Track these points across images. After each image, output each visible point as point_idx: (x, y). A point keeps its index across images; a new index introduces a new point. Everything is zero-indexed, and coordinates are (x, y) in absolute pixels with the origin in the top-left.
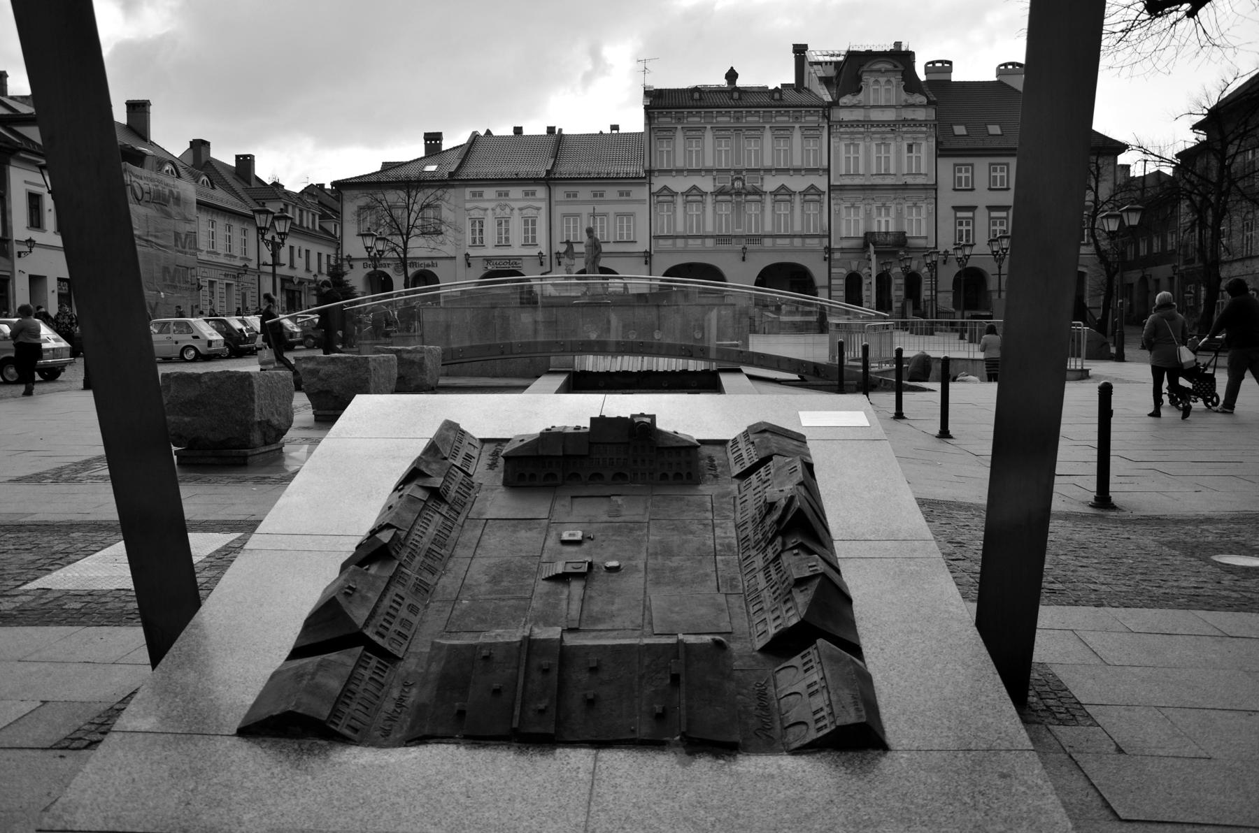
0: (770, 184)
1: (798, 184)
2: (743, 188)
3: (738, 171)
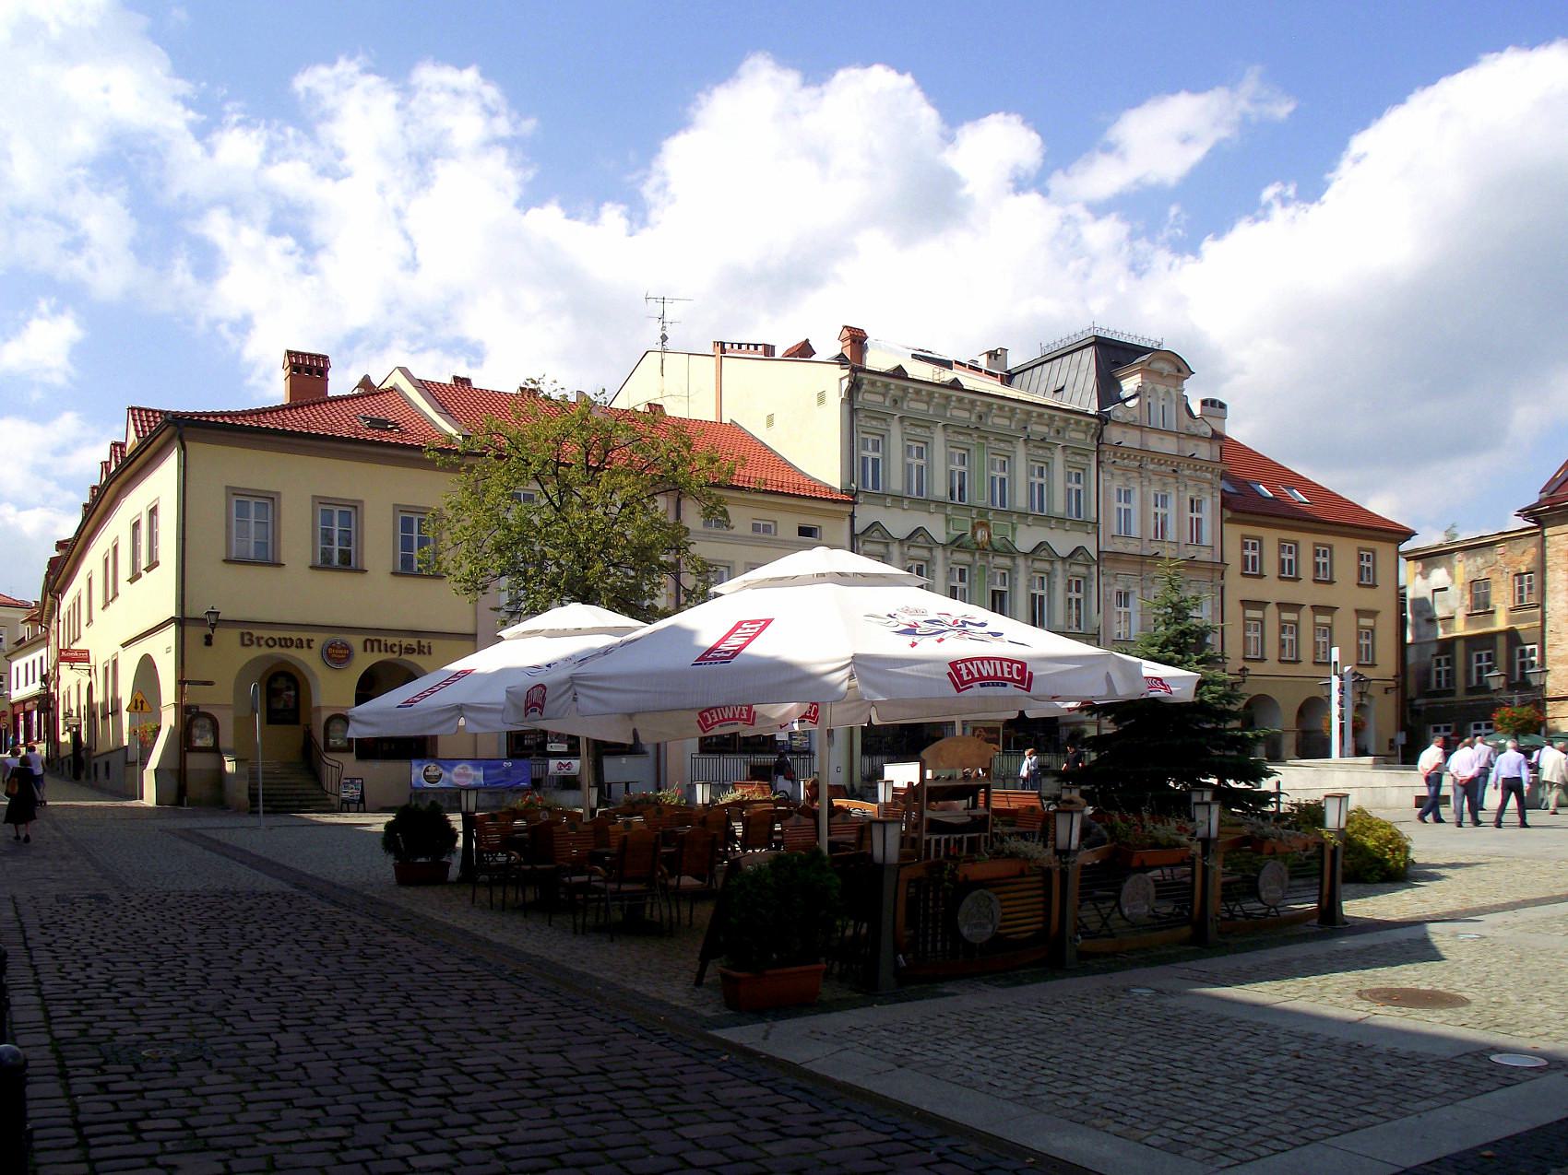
0: (1026, 539)
1: (1063, 542)
2: (990, 542)
3: (983, 511)
